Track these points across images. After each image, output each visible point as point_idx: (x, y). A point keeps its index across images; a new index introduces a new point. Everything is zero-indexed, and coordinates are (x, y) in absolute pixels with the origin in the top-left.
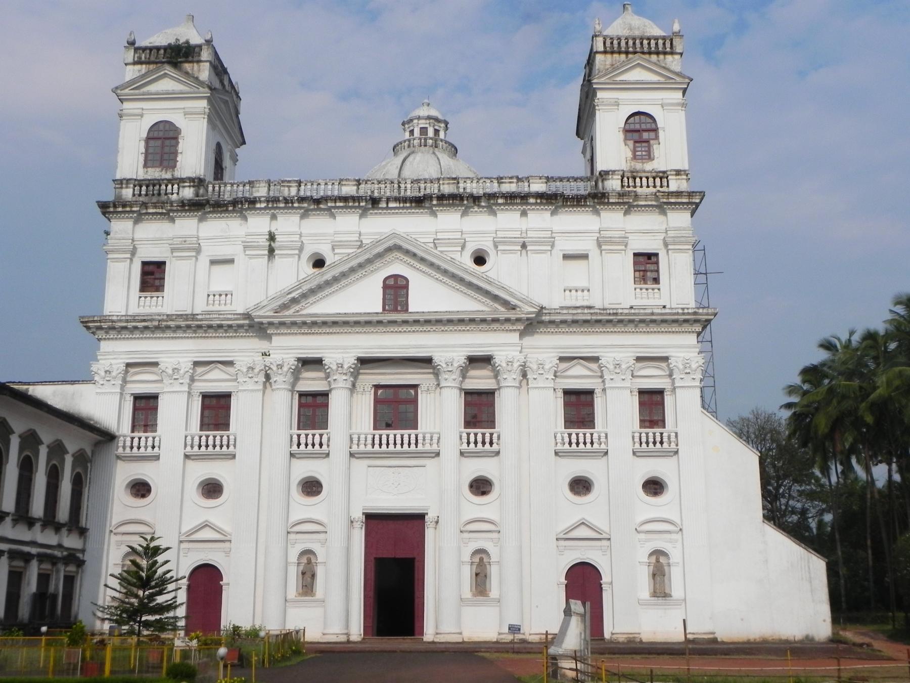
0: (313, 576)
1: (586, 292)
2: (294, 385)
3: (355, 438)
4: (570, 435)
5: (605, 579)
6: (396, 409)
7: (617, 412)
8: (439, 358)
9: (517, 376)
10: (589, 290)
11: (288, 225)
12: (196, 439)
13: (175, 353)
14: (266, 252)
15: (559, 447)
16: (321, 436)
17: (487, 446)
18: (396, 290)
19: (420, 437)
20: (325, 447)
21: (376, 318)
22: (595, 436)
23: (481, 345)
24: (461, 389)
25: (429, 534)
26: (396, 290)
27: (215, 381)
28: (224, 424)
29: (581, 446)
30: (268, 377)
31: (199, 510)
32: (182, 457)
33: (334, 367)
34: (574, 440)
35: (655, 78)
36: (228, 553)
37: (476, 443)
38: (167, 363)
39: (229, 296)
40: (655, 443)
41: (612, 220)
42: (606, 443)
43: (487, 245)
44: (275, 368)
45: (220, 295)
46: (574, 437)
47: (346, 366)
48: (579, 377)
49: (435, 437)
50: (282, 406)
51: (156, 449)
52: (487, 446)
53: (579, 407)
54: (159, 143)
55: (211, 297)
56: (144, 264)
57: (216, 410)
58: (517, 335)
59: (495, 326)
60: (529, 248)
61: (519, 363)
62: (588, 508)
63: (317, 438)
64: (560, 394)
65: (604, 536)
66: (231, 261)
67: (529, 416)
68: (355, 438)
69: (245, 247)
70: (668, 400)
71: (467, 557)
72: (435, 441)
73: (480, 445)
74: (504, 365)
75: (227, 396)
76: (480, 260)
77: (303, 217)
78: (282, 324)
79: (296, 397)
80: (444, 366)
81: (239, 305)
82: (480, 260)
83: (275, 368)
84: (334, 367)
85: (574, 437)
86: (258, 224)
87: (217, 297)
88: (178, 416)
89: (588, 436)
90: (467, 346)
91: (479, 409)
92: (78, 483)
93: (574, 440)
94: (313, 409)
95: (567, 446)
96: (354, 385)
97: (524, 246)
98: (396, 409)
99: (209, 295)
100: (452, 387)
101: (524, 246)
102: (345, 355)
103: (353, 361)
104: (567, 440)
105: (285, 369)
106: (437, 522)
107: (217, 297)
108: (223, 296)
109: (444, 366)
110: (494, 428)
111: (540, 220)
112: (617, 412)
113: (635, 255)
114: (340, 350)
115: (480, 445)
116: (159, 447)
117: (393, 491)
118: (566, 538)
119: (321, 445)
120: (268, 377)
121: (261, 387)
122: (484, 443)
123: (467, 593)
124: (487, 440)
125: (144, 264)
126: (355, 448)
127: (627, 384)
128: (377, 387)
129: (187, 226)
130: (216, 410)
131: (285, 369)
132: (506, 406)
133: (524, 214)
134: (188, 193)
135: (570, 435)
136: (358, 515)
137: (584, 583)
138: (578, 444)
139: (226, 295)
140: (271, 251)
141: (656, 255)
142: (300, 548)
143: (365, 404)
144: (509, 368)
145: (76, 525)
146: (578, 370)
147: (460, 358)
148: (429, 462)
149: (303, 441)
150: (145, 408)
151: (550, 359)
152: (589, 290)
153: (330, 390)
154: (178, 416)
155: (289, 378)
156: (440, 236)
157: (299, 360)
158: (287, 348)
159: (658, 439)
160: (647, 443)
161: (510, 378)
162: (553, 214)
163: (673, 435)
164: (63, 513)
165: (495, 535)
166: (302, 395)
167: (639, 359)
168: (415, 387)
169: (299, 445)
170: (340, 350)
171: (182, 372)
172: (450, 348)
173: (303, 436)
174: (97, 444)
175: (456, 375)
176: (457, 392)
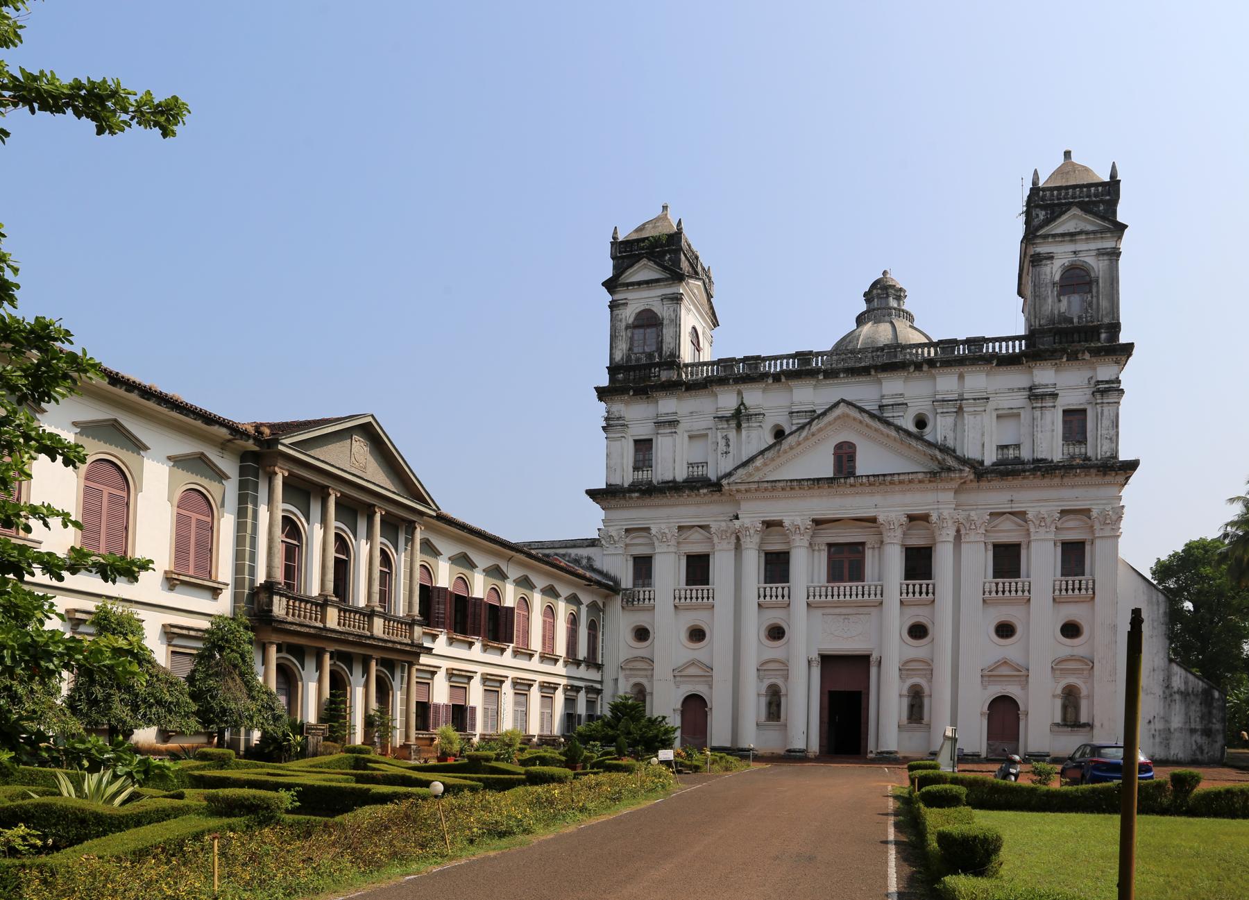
0: (779, 705)
2: (762, 542)
4: (997, 584)
6: (846, 563)
7: (1042, 562)
8: (881, 519)
9: (952, 533)
11: (754, 397)
13: (663, 518)
17: (924, 595)
18: (845, 457)
19: (866, 588)
22: (1020, 585)
25: (873, 671)
26: (845, 457)
28: (705, 580)
29: (1007, 594)
30: (738, 538)
34: (1000, 589)
35: (1090, 228)
36: (711, 687)
37: (914, 593)
40: (1073, 590)
41: (1044, 375)
46: (1000, 585)
48: (1007, 533)
50: (753, 563)
52: (924, 595)
53: (1007, 560)
54: (642, 331)
57: (698, 569)
58: (952, 494)
62: (1010, 649)
63: (780, 590)
64: (990, 547)
65: (1024, 673)
66: (706, 435)
67: (963, 568)
70: (1088, 548)
71: (905, 692)
72: (879, 592)
73: (917, 595)
75: (708, 556)
76: (921, 423)
79: (763, 555)
82: (921, 423)
85: (1000, 585)
86: (727, 400)
88: (669, 572)
91: (919, 564)
92: (593, 627)
93: (1000, 589)
94: (777, 567)
95: (994, 594)
98: (846, 563)
101: (961, 408)
104: (994, 589)
105: (752, 531)
110: (930, 578)
111: (977, 381)
112: (1042, 562)
113: (1064, 411)
115: (917, 595)
118: (989, 676)
120: (738, 538)
122: (921, 593)
124: (924, 590)
125: (636, 441)
126: (811, 598)
127: (1052, 537)
128: (830, 545)
129: (668, 405)
130: (698, 569)
131: (752, 531)
132: (943, 560)
133: (961, 377)
135: (997, 584)
136: (815, 656)
137: (1004, 714)
138: (1003, 592)
141: (1085, 411)
142: (767, 682)
143: (823, 558)
145: (592, 662)
148: (874, 611)
149: (768, 593)
150: (643, 566)
151: (980, 516)
154: (669, 572)
155: (756, 539)
156: (885, 402)
157: (763, 522)
158: (753, 513)
159: (1077, 586)
160: (1067, 590)
163: (1090, 583)
164: (582, 652)
166: (767, 554)
167: (1064, 512)
168: (863, 544)
170: (797, 512)
173: (768, 590)
174: (607, 597)
175: (899, 533)
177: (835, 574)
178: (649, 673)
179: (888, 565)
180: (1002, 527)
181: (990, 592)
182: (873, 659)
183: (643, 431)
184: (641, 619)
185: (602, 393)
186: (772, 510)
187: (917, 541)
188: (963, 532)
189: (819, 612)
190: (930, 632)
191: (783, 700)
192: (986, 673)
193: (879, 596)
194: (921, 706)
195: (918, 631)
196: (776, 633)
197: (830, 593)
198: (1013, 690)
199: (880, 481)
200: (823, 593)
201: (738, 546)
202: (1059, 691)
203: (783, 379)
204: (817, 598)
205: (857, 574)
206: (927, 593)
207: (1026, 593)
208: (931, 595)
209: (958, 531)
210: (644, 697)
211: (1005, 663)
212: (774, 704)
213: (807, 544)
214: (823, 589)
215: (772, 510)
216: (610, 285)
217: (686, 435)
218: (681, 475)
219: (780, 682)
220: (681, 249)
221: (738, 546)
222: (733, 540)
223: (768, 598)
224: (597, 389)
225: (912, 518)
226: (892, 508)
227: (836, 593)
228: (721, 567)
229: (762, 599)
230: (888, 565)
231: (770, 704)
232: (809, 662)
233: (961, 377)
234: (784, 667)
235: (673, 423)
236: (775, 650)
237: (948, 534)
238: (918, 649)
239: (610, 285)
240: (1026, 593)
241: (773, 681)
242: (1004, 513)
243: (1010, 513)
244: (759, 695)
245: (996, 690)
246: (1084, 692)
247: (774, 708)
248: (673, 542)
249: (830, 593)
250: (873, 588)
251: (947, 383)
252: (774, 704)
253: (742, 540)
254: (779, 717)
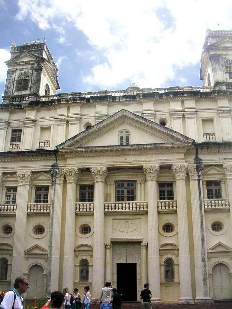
0: (87, 272)
1: (214, 136)
3: (107, 205)
6: (127, 192)
10: (215, 135)
11: (75, 111)
12: (32, 206)
13: (24, 168)
14: (65, 123)
15: (206, 207)
16: (90, 204)
17: (171, 208)
19: (138, 204)
20: (92, 210)
21: (115, 148)
23: (166, 160)
24: (157, 182)
30: (65, 178)
31: (34, 241)
32: (26, 215)
33: (96, 172)
38: (20, 172)
39: (49, 143)
42: (229, 205)
43: (166, 115)
44: (68, 174)
45: (45, 143)
47: (101, 172)
49: (145, 204)
51: (15, 211)
55: (41, 143)
57: (41, 194)
59: (172, 150)
60: (186, 116)
61: (184, 168)
63: (88, 205)
68: (107, 205)
69: (56, 121)
71: (163, 263)
74: (178, 169)
77: (82, 107)
78: (72, 152)
79: (79, 187)
80: (149, 170)
83: (68, 174)
84: (96, 172)
86: (62, 112)
87: (43, 143)
90: (160, 160)
91: (166, 191)
94: (86, 193)
96: (105, 181)
97: (184, 116)
99: (40, 143)
100: (153, 180)
102: (101, 166)
103: (104, 168)
105: (73, 174)
106: (147, 246)
107: (43, 143)
108: (46, 143)
109: (149, 170)
114: (98, 165)
116: (16, 210)
119: (90, 209)
121: (62, 182)
123: (164, 281)
124: (171, 205)
126: (106, 210)
128: (116, 181)
129: (31, 114)
130: (41, 194)
131: (73, 174)
132: (180, 188)
133: (183, 102)
136: (109, 242)
139: (47, 142)
140: (68, 122)
142: (80, 258)
144: (180, 170)
146: (213, 172)
147: (156, 165)
149: (81, 207)
152: (215, 135)
153: (94, 184)
155: (75, 178)
156: (144, 112)
157: (79, 169)
161: (181, 176)
162: (196, 101)
165: (176, 252)
168: (135, 181)
170: (98, 165)
171: (26, 176)
172: (152, 162)
175: (155, 175)
176: (155, 183)
177: (119, 198)
178: (10, 252)
179: (148, 194)
180: (210, 172)
181: (208, 206)
182: (144, 242)
184: (9, 221)
186: (85, 162)
187: (166, 179)
188: (190, 174)
189: (110, 219)
190: (175, 229)
191: (90, 269)
192: (210, 251)
193: (145, 209)
195: (168, 228)
196: (86, 229)
199: (143, 149)
200: (113, 207)
201: (65, 182)
203: (91, 102)
204: (110, 210)
205: (132, 197)
206: (173, 207)
207: (227, 206)
208: (175, 208)
209: (188, 174)
210: (7, 265)
213: (104, 181)
215: (85, 162)
216: (9, 63)
217: (39, 129)
218: (36, 148)
220: (44, 49)
221: (65, 182)
222: (62, 178)
223: (81, 210)
225: (162, 167)
226: (152, 162)
229: (78, 210)
230: (148, 194)
231: (82, 271)
232: (106, 246)
233: (183, 102)
234: (90, 250)
236: (84, 240)
237: (181, 176)
238: (169, 238)
239: (9, 63)
240: (227, 206)
241: (85, 257)
242: (210, 165)
243: (214, 165)
244: (75, 266)
247: (85, 274)
248: (29, 180)
250: (142, 204)
251: (175, 105)
253: (67, 178)
254: (87, 279)
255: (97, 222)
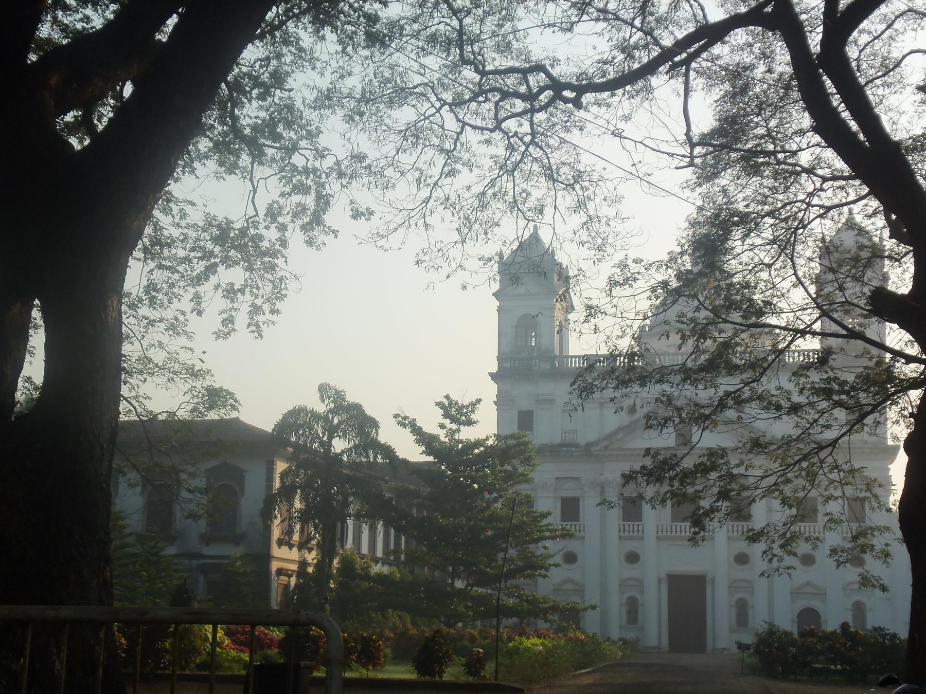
0: (637, 612)
5: (823, 619)
22: (817, 528)
25: (709, 588)
27: (569, 491)
30: (603, 488)
56: (520, 412)
63: (636, 527)
81: (582, 441)
89: (812, 528)
117: (687, 560)
118: (796, 594)
119: (638, 531)
120: (603, 488)
125: (520, 412)
126: (660, 533)
134: (546, 366)
136: (663, 575)
149: (627, 528)
169: (624, 531)
183: (525, 405)
185: (493, 376)
194: (747, 615)
196: (633, 558)
197: (674, 530)
198: (816, 604)
200: (669, 530)
202: (849, 606)
204: (665, 533)
211: (809, 584)
212: (633, 610)
214: (669, 527)
218: (557, 440)
219: (636, 595)
223: (626, 533)
224: (490, 374)
227: (678, 530)
228: (589, 509)
229: (622, 533)
231: (629, 611)
232: (659, 581)
234: (640, 583)
235: (551, 401)
236: (630, 571)
245: (802, 604)
246: (869, 605)
249: (674, 530)
252: (633, 610)
255: (649, 548)
